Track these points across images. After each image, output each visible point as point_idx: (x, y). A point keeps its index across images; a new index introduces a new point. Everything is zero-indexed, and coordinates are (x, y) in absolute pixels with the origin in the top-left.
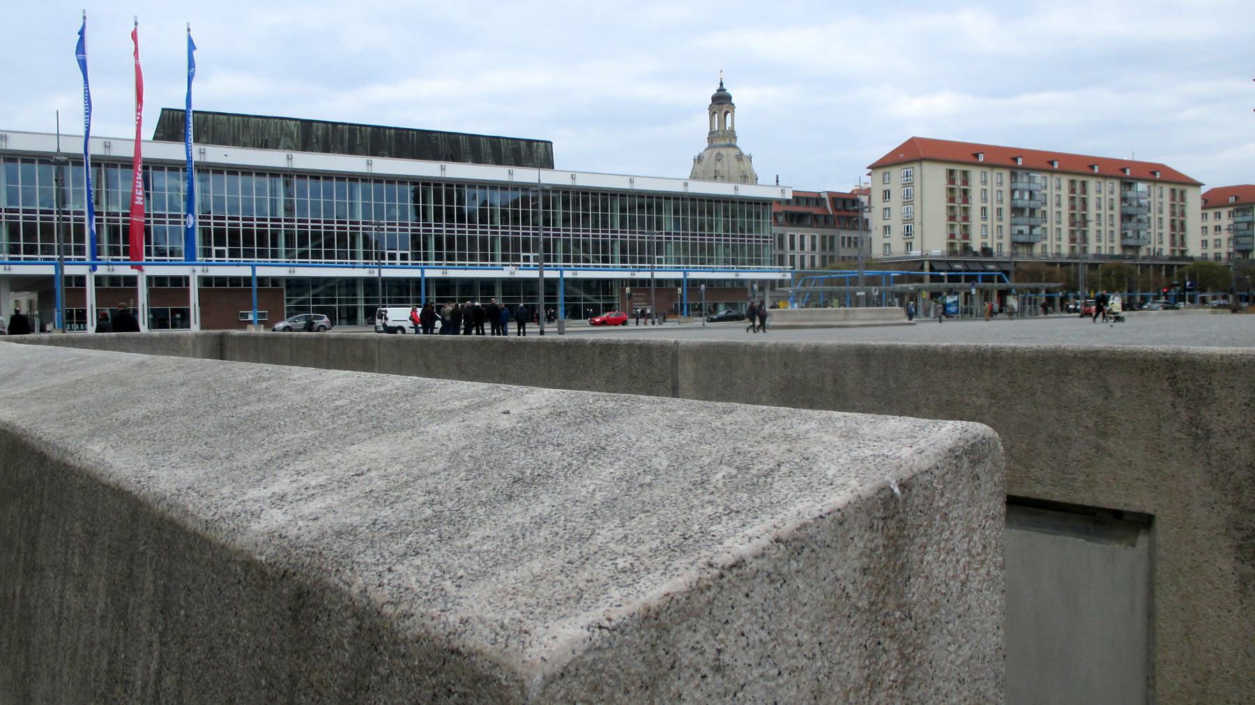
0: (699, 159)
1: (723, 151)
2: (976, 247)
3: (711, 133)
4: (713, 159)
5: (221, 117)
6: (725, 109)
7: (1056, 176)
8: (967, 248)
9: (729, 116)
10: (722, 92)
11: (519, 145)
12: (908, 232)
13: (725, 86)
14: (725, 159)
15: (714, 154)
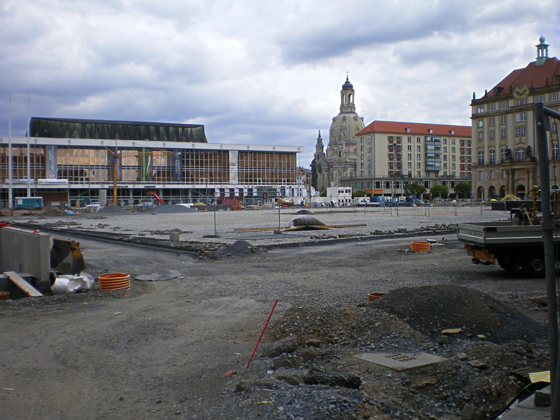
0: (334, 120)
1: (346, 115)
2: (405, 173)
3: (341, 106)
4: (341, 120)
5: (52, 121)
6: (349, 92)
7: (452, 138)
8: (399, 174)
9: (351, 96)
10: (347, 84)
11: (178, 129)
12: (370, 166)
13: (349, 80)
14: (347, 120)
15: (342, 117)
